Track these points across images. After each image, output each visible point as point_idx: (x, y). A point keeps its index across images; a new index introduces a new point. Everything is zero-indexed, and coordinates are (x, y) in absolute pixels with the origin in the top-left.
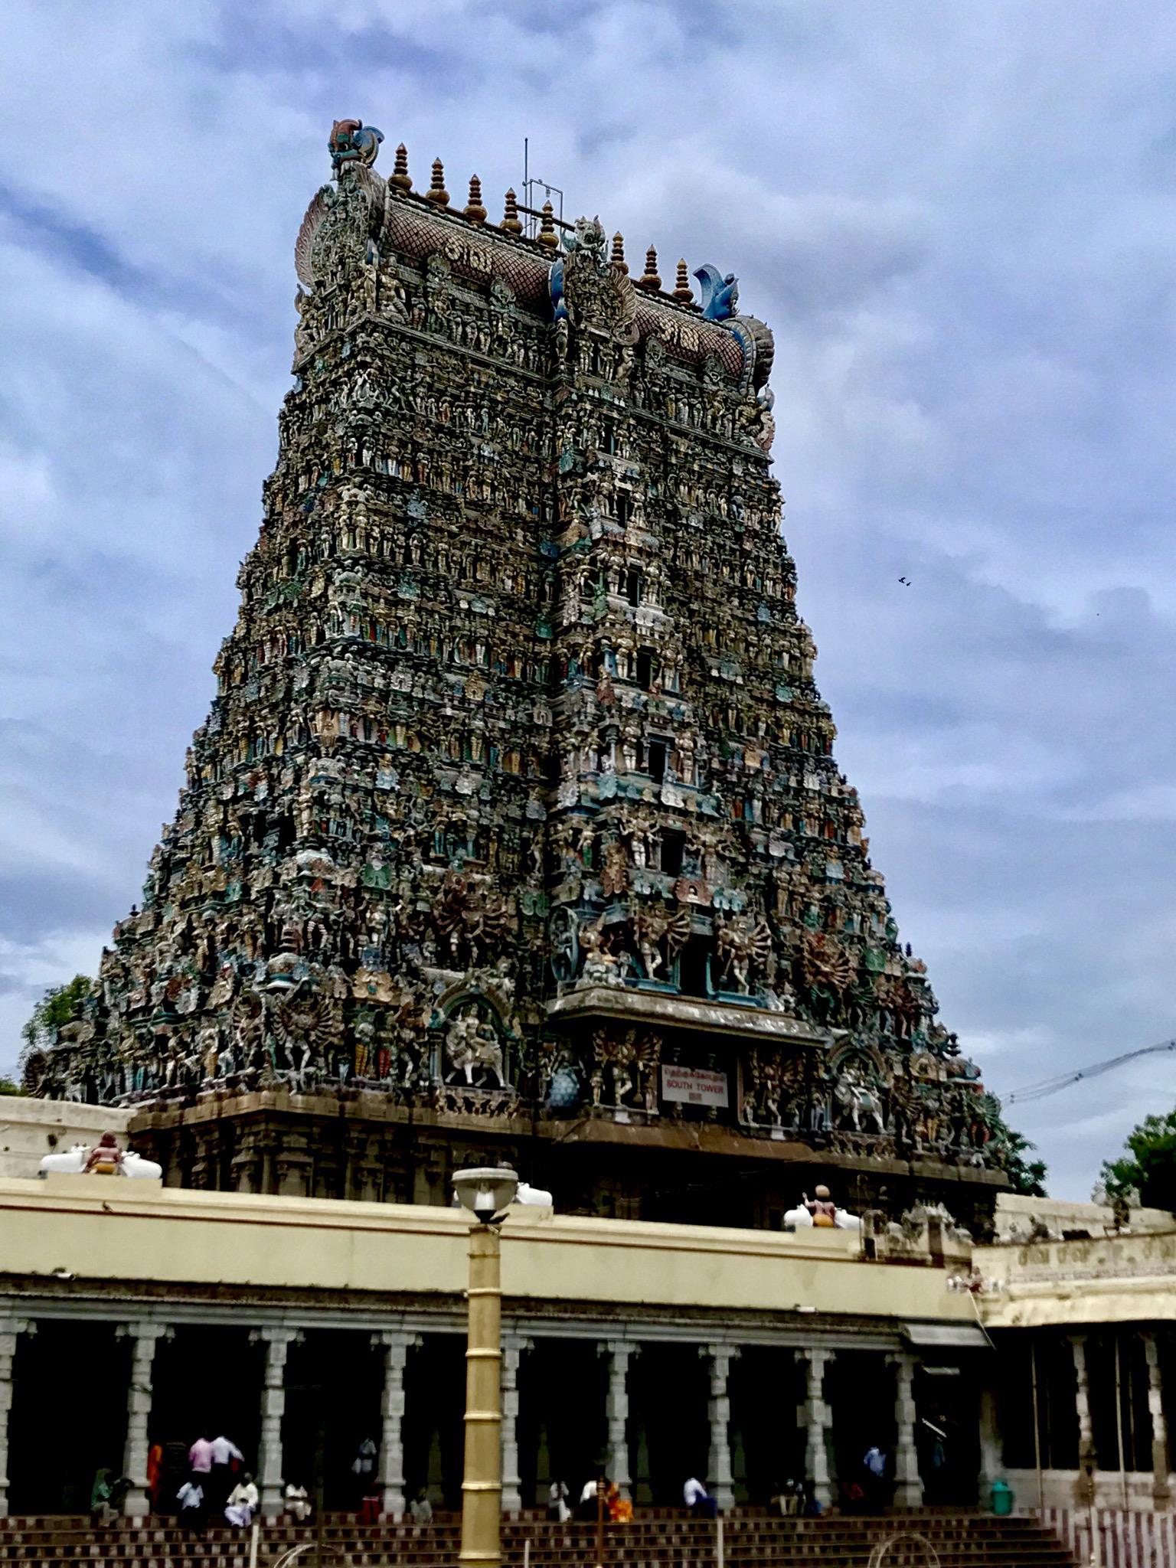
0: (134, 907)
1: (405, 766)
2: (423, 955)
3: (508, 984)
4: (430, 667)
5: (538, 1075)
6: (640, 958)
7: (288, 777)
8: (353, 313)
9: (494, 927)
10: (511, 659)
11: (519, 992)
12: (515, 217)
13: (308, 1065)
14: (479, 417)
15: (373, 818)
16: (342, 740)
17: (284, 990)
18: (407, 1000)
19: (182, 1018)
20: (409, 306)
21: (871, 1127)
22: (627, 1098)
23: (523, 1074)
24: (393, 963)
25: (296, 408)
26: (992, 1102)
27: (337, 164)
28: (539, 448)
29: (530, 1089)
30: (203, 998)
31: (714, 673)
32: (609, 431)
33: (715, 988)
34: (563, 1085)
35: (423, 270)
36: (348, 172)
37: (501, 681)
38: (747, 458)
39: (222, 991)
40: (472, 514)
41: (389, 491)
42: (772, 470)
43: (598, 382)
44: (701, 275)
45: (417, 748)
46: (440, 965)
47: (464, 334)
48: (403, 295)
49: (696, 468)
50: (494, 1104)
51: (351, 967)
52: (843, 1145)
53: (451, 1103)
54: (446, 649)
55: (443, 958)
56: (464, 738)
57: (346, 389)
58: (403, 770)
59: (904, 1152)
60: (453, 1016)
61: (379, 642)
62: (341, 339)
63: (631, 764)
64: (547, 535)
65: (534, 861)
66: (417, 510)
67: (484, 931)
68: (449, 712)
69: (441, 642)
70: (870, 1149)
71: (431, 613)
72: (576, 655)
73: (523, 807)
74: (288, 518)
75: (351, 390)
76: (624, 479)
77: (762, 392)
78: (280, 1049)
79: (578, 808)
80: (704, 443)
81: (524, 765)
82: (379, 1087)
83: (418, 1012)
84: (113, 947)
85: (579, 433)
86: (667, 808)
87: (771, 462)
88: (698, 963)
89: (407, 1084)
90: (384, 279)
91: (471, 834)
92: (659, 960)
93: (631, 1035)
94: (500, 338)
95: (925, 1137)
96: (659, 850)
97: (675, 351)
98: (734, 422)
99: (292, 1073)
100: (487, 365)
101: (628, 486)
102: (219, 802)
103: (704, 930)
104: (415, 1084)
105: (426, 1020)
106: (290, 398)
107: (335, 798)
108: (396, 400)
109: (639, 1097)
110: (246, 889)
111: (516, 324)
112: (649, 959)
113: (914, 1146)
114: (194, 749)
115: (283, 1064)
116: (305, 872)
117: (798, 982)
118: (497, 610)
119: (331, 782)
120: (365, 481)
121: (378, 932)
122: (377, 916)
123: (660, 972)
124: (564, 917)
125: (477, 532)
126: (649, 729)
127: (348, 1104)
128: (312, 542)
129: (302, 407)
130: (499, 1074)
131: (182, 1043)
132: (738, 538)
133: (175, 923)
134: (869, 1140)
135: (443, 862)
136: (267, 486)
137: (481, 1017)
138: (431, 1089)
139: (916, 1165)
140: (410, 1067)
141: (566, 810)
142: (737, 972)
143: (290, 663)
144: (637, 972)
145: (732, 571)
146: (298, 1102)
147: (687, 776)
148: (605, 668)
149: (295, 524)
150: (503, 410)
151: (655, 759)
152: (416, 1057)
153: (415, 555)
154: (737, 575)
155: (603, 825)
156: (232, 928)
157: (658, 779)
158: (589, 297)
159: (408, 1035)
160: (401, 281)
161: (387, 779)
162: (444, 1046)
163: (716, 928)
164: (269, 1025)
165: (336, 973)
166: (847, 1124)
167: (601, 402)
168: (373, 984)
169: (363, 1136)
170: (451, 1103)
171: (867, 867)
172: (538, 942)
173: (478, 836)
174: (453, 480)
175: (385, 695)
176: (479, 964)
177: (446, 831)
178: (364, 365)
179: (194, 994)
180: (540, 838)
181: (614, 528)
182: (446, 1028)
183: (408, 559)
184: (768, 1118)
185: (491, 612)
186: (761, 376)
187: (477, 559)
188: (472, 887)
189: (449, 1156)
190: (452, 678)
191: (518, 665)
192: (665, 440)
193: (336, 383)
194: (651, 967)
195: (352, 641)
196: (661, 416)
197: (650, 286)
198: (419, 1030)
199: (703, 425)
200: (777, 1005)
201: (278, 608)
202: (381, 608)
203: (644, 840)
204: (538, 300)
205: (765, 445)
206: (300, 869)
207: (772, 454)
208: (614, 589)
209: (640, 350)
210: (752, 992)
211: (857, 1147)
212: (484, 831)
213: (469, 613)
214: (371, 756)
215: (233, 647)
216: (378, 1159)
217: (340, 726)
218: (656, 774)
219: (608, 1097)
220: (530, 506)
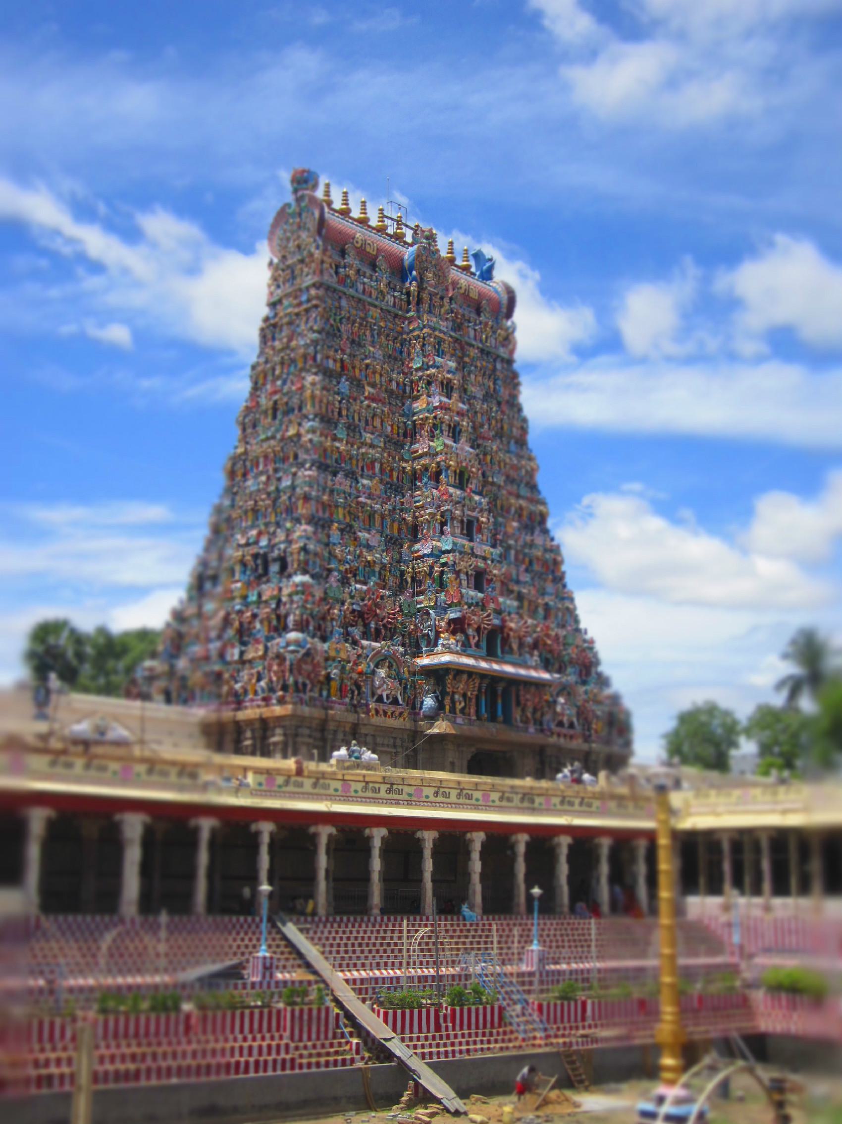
2: (356, 632)
5: (415, 697)
6: (467, 637)
9: (392, 619)
10: (392, 470)
13: (311, 690)
14: (372, 336)
17: (297, 652)
19: (228, 663)
20: (337, 273)
21: (571, 726)
22: (462, 711)
26: (628, 714)
27: (295, 191)
28: (401, 352)
30: (242, 653)
31: (490, 479)
32: (439, 344)
33: (503, 652)
35: (343, 253)
37: (387, 483)
45: (348, 520)
47: (364, 289)
48: (334, 266)
50: (397, 713)
54: (360, 465)
55: (365, 635)
56: (371, 516)
58: (342, 531)
59: (587, 739)
60: (377, 666)
61: (329, 462)
65: (407, 582)
69: (358, 461)
72: (426, 469)
76: (449, 372)
77: (509, 323)
79: (431, 555)
80: (482, 351)
81: (400, 530)
82: (342, 704)
86: (476, 556)
89: (355, 702)
91: (377, 569)
93: (465, 677)
94: (382, 292)
95: (596, 731)
96: (473, 579)
98: (496, 339)
99: (301, 695)
100: (376, 306)
101: (449, 376)
103: (496, 622)
104: (359, 702)
105: (362, 667)
106: (266, 319)
107: (311, 547)
108: (332, 326)
109: (467, 710)
112: (471, 638)
113: (590, 736)
118: (385, 444)
121: (336, 620)
122: (336, 611)
123: (477, 645)
124: (428, 614)
128: (287, 403)
129: (275, 326)
134: (571, 732)
135: (365, 583)
137: (390, 667)
140: (356, 693)
141: (424, 556)
144: (466, 645)
145: (497, 422)
146: (306, 710)
148: (442, 477)
151: (469, 528)
152: (359, 687)
153: (344, 413)
155: (445, 564)
156: (254, 616)
157: (471, 540)
162: (373, 681)
163: (503, 621)
164: (291, 671)
166: (560, 724)
167: (434, 329)
170: (377, 712)
171: (564, 586)
172: (412, 627)
173: (381, 569)
174: (361, 370)
177: (365, 566)
180: (410, 570)
182: (374, 673)
183: (340, 414)
184: (526, 721)
185: (382, 445)
186: (509, 314)
187: (374, 415)
188: (382, 598)
191: (395, 474)
193: (297, 315)
194: (473, 642)
199: (481, 341)
203: (467, 574)
205: (512, 352)
208: (446, 433)
211: (565, 736)
212: (383, 567)
215: (235, 459)
218: (470, 537)
219: (453, 710)
220: (398, 384)
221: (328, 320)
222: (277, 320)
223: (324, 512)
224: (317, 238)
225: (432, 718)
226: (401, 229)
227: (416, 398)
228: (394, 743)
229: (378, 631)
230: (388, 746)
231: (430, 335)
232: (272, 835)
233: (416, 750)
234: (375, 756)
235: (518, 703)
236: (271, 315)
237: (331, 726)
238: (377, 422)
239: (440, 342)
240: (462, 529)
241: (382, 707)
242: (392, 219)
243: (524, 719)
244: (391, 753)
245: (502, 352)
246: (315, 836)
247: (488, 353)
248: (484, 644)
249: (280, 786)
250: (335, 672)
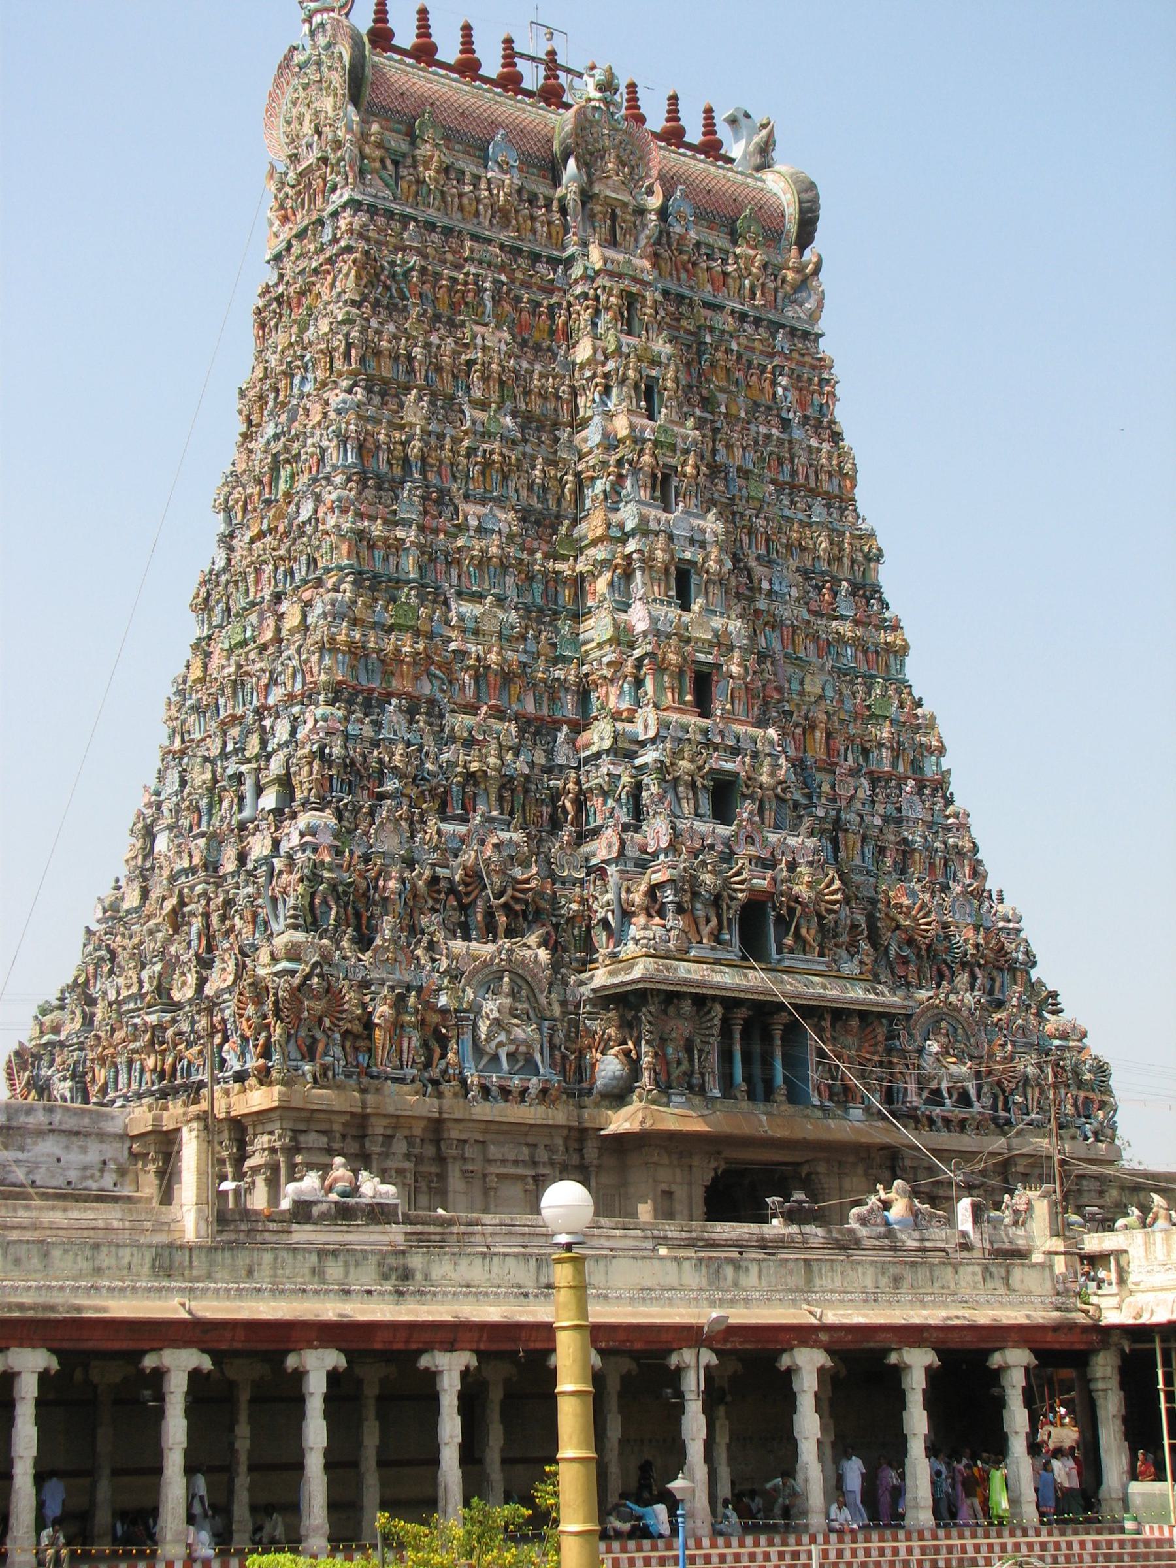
0: (117, 880)
3: (543, 955)
7: (282, 731)
8: (334, 189)
11: (555, 965)
12: (515, 65)
15: (381, 773)
17: (293, 973)
21: (964, 1099)
23: (564, 1057)
34: (609, 1066)
35: (413, 139)
36: (322, 25)
38: (793, 332)
39: (220, 979)
40: (481, 416)
41: (383, 394)
44: (733, 121)
49: (734, 346)
57: (330, 278)
62: (321, 222)
65: (566, 813)
67: (513, 897)
71: (436, 531)
73: (550, 753)
74: (270, 430)
75: (335, 279)
77: (808, 255)
85: (597, 312)
87: (822, 335)
88: (756, 925)
90: (367, 150)
92: (714, 922)
102: (206, 759)
106: (267, 289)
110: (242, 858)
111: (519, 191)
112: (702, 921)
114: (173, 699)
116: (307, 839)
117: (874, 938)
120: (355, 384)
122: (392, 884)
127: (370, 1098)
129: (279, 299)
130: (538, 1058)
133: (164, 898)
134: (960, 1113)
135: (464, 820)
136: (242, 394)
139: (1015, 1142)
142: (804, 931)
143: (278, 598)
149: (276, 437)
150: (508, 293)
154: (787, 468)
156: (229, 903)
160: (387, 149)
162: (475, 1027)
166: (936, 1097)
169: (389, 1132)
170: (485, 1091)
171: (949, 801)
174: (455, 377)
178: (349, 249)
179: (191, 979)
180: (571, 786)
189: (484, 1152)
196: (691, 288)
197: (674, 136)
200: (850, 967)
201: (261, 535)
203: (693, 785)
205: (814, 316)
206: (302, 835)
207: (821, 326)
210: (821, 955)
215: (211, 579)
216: (407, 1156)
221: (377, 275)
222: (281, 289)
224: (351, 108)
225: (619, 1096)
226: (557, 77)
227: (584, 423)
228: (532, 1156)
230: (516, 1162)
232: (44, 1378)
234: (391, 1189)
236: (273, 280)
237: (378, 1127)
239: (631, 300)
242: (533, 59)
244: (522, 1178)
246: (159, 1375)
248: (732, 936)
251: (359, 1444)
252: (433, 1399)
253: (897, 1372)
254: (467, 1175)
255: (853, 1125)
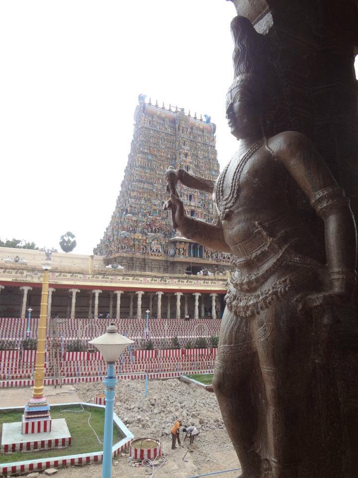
1: (146, 200)
4: (151, 183)
16: (135, 196)
18: (145, 238)
21: (229, 258)
22: (183, 254)
24: (143, 233)
25: (133, 141)
29: (166, 252)
30: (113, 239)
34: (172, 252)
38: (211, 146)
40: (160, 157)
42: (216, 148)
43: (183, 134)
44: (205, 116)
45: (149, 197)
46: (151, 232)
51: (135, 233)
52: (223, 261)
53: (152, 255)
55: (152, 232)
63: (186, 198)
64: (173, 161)
66: (150, 157)
68: (154, 191)
70: (228, 262)
76: (187, 150)
78: (122, 246)
80: (204, 144)
83: (146, 240)
84: (106, 231)
91: (158, 211)
97: (198, 128)
105: (148, 241)
107: (133, 205)
109: (185, 254)
110: (121, 222)
115: (122, 248)
119: (133, 203)
125: (161, 160)
126: (189, 192)
127: (134, 255)
131: (110, 246)
132: (209, 160)
134: (228, 260)
137: (157, 240)
138: (148, 253)
143: (129, 184)
146: (125, 255)
147: (196, 200)
152: (146, 247)
153: (149, 165)
157: (190, 201)
158: (182, 120)
159: (144, 244)
161: (143, 202)
165: (132, 234)
166: (224, 258)
168: (138, 236)
170: (152, 255)
175: (143, 188)
176: (158, 232)
181: (184, 159)
182: (151, 243)
183: (148, 165)
186: (214, 132)
190: (155, 185)
192: (196, 144)
195: (138, 180)
198: (146, 243)
202: (143, 174)
204: (173, 121)
209: (192, 129)
211: (226, 261)
212: (160, 211)
213: (159, 174)
214: (140, 199)
217: (135, 194)
223: (140, 194)
225: (173, 256)
229: (155, 230)
231: (181, 140)
233: (170, 266)
235: (205, 251)
238: (162, 167)
240: (187, 198)
241: (153, 253)
243: (207, 256)
245: (211, 144)
247: (206, 145)
249: (57, 276)
250: (137, 243)
251: (109, 304)
252: (22, 296)
253: (194, 297)
254: (149, 267)
255: (210, 261)
